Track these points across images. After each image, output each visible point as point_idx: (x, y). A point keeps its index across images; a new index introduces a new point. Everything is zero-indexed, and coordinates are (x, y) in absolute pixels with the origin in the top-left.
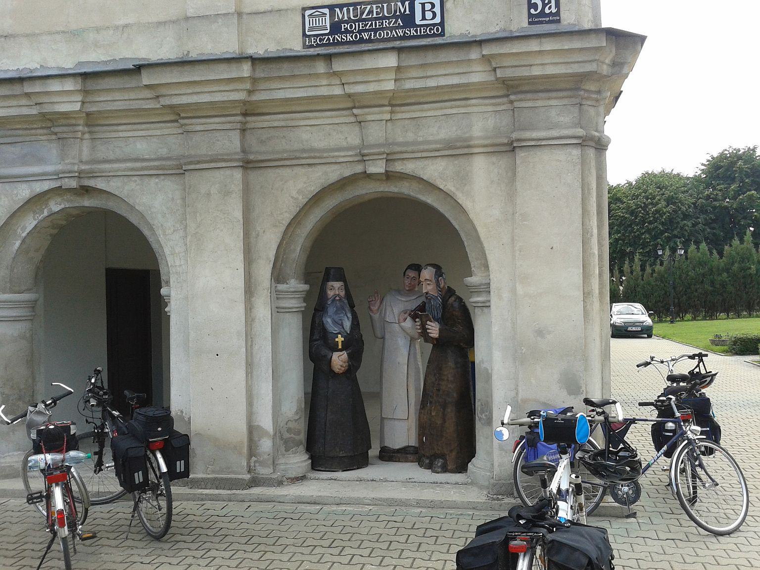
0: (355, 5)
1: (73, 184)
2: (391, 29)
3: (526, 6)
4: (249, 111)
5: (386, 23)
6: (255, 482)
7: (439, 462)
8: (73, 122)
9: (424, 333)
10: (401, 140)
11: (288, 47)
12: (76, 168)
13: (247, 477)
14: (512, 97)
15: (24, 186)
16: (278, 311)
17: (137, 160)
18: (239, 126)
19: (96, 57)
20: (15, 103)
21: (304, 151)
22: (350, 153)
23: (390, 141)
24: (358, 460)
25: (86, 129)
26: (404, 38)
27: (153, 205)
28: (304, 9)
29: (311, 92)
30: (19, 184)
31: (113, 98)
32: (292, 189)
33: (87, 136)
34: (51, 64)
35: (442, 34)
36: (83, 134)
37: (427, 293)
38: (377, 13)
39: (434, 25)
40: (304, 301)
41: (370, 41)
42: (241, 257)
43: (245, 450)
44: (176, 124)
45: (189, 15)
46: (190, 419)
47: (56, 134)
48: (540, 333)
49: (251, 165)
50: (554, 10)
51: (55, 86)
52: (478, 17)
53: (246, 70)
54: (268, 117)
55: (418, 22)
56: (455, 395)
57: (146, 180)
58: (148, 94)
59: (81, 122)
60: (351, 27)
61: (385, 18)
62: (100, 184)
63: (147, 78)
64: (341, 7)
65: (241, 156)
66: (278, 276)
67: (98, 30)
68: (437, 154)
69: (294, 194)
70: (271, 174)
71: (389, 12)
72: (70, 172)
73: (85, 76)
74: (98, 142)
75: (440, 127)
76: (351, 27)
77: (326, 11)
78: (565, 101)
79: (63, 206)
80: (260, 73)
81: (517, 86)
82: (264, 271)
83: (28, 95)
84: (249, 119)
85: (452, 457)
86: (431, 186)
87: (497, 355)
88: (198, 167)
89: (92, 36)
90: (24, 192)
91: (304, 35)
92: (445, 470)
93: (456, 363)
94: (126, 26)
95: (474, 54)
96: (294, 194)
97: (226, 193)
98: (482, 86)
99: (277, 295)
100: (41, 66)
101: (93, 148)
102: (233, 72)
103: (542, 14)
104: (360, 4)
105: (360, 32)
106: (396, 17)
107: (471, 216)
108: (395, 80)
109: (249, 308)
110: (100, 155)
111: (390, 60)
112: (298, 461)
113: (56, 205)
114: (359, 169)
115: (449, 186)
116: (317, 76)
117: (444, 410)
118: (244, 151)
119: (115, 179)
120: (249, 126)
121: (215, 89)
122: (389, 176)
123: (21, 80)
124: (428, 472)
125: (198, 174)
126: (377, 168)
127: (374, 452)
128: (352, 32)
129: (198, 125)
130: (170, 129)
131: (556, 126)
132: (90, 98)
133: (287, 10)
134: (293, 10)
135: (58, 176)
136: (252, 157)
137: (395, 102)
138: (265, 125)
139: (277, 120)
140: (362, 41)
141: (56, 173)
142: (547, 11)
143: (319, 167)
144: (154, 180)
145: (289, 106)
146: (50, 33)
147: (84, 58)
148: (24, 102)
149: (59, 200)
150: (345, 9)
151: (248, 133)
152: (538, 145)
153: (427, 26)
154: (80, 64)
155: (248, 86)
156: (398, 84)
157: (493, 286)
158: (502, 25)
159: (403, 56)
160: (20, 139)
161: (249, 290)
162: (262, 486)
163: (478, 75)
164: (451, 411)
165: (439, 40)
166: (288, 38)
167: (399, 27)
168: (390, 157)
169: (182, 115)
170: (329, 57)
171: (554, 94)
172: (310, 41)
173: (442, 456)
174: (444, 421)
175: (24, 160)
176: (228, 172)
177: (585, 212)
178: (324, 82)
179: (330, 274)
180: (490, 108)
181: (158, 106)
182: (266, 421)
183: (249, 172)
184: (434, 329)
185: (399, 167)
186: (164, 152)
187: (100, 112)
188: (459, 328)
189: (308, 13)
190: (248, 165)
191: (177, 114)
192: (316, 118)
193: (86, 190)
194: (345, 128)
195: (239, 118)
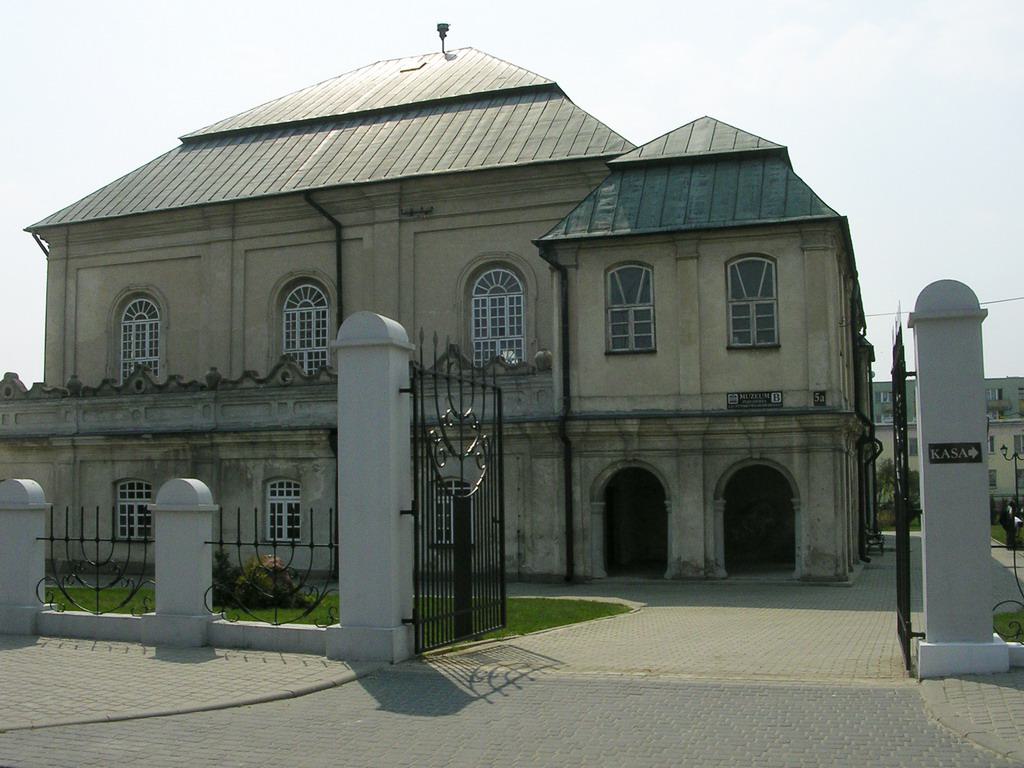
4: (705, 433)
27: (665, 468)
28: (728, 394)
31: (653, 426)
32: (722, 465)
51: (629, 422)
55: (773, 400)
62: (643, 459)
66: (716, 498)
67: (642, 397)
82: (710, 496)
86: (778, 464)
94: (654, 396)
95: (793, 418)
111: (762, 419)
115: (785, 464)
122: (761, 459)
126: (757, 456)
139: (718, 437)
145: (722, 433)
161: (705, 503)
163: (795, 425)
177: (835, 477)
185: (765, 456)
191: (676, 434)
193: (635, 460)
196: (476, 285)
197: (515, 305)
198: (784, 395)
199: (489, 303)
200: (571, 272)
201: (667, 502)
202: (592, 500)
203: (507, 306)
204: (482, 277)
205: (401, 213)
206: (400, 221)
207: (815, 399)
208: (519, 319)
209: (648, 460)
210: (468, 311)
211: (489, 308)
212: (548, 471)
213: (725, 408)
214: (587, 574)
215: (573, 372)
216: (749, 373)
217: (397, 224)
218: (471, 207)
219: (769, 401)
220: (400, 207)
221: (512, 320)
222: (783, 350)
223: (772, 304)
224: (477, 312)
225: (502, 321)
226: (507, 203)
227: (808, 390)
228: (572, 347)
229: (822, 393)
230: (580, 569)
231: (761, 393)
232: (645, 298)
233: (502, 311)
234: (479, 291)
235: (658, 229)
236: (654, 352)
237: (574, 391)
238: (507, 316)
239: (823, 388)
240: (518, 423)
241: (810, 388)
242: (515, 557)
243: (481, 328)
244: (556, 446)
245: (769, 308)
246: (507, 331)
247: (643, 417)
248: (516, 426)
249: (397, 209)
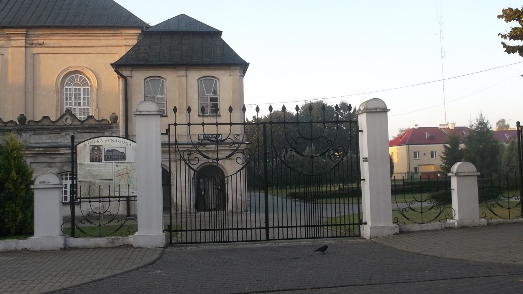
115: (222, 164)
122: (212, 162)
196: (66, 81)
197: (86, 92)
199: (73, 90)
200: (129, 78)
203: (82, 92)
205: (26, 43)
206: (26, 47)
208: (88, 98)
210: (62, 93)
211: (73, 92)
213: (197, 141)
215: (129, 124)
217: (24, 48)
218: (64, 43)
220: (25, 40)
221: (84, 98)
223: (217, 98)
224: (67, 94)
225: (80, 99)
226: (82, 43)
229: (238, 135)
232: (162, 93)
233: (79, 94)
234: (67, 84)
235: (169, 63)
236: (166, 116)
238: (82, 97)
239: (238, 133)
243: (69, 101)
245: (216, 100)
246: (82, 103)
249: (24, 41)
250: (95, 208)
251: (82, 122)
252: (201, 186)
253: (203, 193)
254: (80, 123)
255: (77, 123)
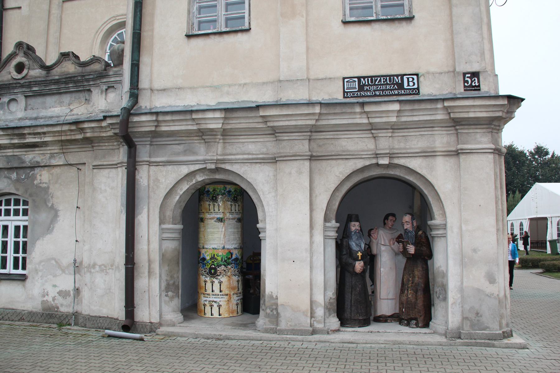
0: (372, 77)
1: (213, 166)
2: (391, 90)
3: (462, 82)
4: (314, 130)
5: (388, 87)
6: (314, 332)
7: (414, 322)
8: (215, 133)
9: (405, 252)
10: (397, 147)
11: (335, 97)
12: (215, 158)
13: (311, 329)
14: (457, 127)
15: (184, 167)
16: (326, 237)
17: (249, 154)
18: (308, 138)
19: (230, 99)
20: (185, 123)
21: (344, 151)
22: (369, 153)
23: (391, 147)
24: (365, 323)
25: (221, 137)
26: (398, 95)
28: (344, 79)
29: (350, 121)
30: (182, 166)
31: (239, 123)
33: (221, 141)
34: (202, 103)
35: (418, 94)
36: (220, 139)
37: (406, 229)
38: (384, 82)
39: (414, 89)
40: (337, 232)
41: (380, 96)
42: (308, 207)
43: (309, 314)
44: (272, 136)
45: (281, 79)
46: (277, 296)
47: (204, 140)
48: (475, 251)
49: (313, 158)
50: (477, 84)
51: (210, 115)
52: (437, 86)
53: (317, 110)
54: (324, 133)
55: (405, 87)
56: (423, 285)
57: (254, 165)
58: (260, 120)
59: (219, 134)
60: (370, 88)
61: (387, 84)
62: (228, 167)
63: (262, 113)
64: (364, 78)
65: (309, 153)
66: (326, 219)
67: (230, 86)
68: (417, 155)
69: (337, 174)
70: (324, 163)
71: (390, 81)
72: (212, 160)
73: (226, 110)
74: (227, 144)
75: (418, 141)
76: (370, 88)
77: (356, 80)
78: (484, 130)
79: (204, 178)
80: (324, 111)
81: (460, 122)
83: (193, 119)
84: (313, 134)
85: (421, 319)
87: (451, 263)
88: (285, 159)
89: (226, 89)
90: (185, 170)
91: (344, 92)
92: (417, 326)
93: (423, 268)
94: (245, 84)
95: (440, 106)
96: (337, 174)
97: (300, 173)
98: (441, 121)
99: (325, 229)
100: (197, 104)
101: (224, 148)
102: (310, 110)
103: (471, 86)
104: (375, 77)
105: (374, 91)
106: (394, 84)
107: (436, 188)
108: (397, 117)
109: (311, 236)
110: (228, 151)
111: (396, 107)
112: (334, 322)
113: (200, 178)
114: (374, 161)
116: (355, 113)
117: (416, 293)
118: (309, 151)
119: (236, 164)
120: (313, 137)
121: (299, 118)
122: (390, 166)
123: (192, 112)
124: (407, 328)
125: (284, 162)
126: (384, 161)
127: (372, 318)
128: (370, 91)
129: (285, 137)
130: (270, 138)
131: (480, 143)
132: (227, 122)
133: (334, 78)
134: (338, 78)
135: (205, 161)
136: (314, 154)
137: (394, 128)
138: (322, 137)
140: (375, 95)
141: (204, 160)
142: (473, 84)
143: (352, 160)
144: (258, 165)
145: (337, 129)
146: (203, 87)
147: (221, 100)
148: (190, 123)
149: (202, 175)
150: (366, 79)
151: (312, 142)
152: (471, 152)
153: (410, 89)
154: (219, 103)
155: (317, 118)
156: (398, 118)
157: (449, 225)
158: (449, 90)
159: (402, 105)
160: (183, 142)
161: (312, 227)
162: (319, 334)
163: (440, 116)
164: (420, 294)
165: (416, 97)
166: (336, 94)
167: (396, 89)
168: (391, 156)
169: (277, 131)
170: (362, 104)
171: (479, 127)
172: (347, 95)
173: (415, 319)
174: (416, 299)
175: (185, 152)
176: (302, 162)
178: (358, 116)
179: (350, 218)
180: (445, 132)
181: (265, 126)
182: (320, 298)
183: (312, 162)
184: (412, 249)
185: (396, 161)
186: (264, 150)
187: (231, 128)
188: (424, 248)
189: (346, 80)
190: (312, 158)
191: (274, 132)
192: (351, 134)
194: (366, 140)
195: (309, 134)
196: (110, 42)
198: (421, 79)
201: (258, 226)
202: (161, 222)
204: (116, 35)
207: (465, 81)
209: (235, 168)
212: (110, 185)
214: (153, 321)
215: (145, 59)
216: (375, 52)
219: (400, 86)
222: (414, 22)
227: (454, 71)
228: (146, 28)
229: (475, 75)
230: (145, 313)
231: (390, 76)
237: (144, 83)
240: (76, 123)
241: (457, 70)
242: (72, 293)
244: (122, 154)
247: (229, 111)
248: (73, 127)
250: (60, 293)
251: (48, 69)
252: (353, 245)
253: (359, 266)
254: (44, 73)
255: (36, 73)
